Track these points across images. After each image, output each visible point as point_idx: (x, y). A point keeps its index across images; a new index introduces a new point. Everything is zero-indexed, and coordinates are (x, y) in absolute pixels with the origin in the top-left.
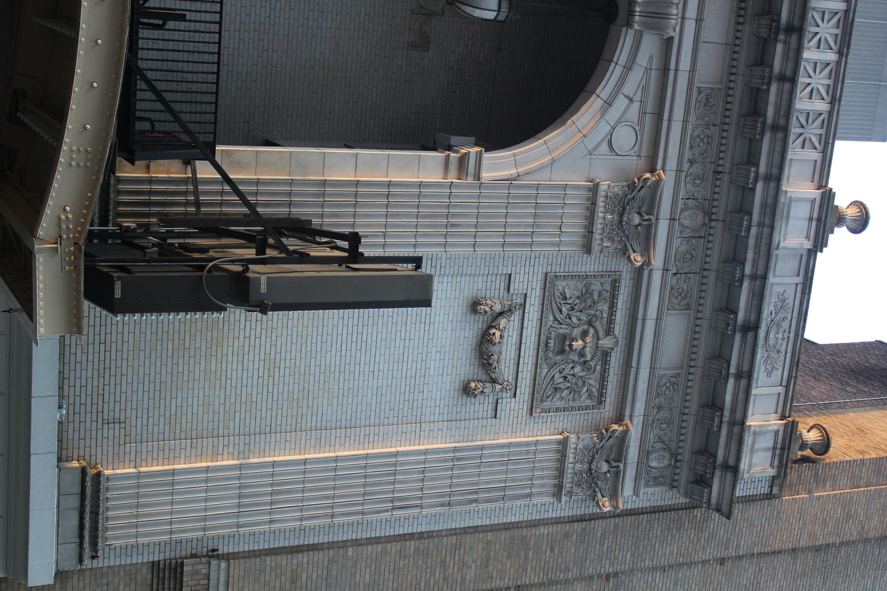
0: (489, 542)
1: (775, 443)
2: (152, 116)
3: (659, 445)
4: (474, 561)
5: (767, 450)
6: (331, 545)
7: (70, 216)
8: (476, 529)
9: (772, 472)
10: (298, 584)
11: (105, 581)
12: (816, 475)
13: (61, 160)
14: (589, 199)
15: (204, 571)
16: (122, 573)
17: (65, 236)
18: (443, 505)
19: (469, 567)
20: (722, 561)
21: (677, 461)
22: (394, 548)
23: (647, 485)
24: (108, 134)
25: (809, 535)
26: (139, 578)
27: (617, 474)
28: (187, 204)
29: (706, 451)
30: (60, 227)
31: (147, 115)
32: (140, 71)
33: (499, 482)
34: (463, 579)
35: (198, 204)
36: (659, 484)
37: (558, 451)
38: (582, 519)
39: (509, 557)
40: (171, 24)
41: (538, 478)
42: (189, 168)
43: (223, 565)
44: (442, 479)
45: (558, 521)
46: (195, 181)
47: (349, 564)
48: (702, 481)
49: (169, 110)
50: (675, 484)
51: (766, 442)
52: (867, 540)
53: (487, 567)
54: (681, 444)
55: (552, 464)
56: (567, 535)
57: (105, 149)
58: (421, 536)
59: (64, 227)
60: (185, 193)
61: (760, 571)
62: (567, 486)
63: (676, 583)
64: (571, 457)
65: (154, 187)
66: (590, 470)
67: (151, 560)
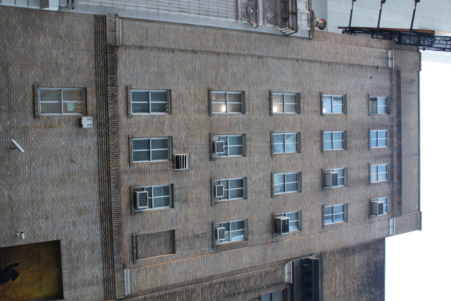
0: (215, 33)
1: (308, 18)
3: (269, 9)
4: (211, 39)
5: (306, 20)
6: (159, 22)
8: (210, 27)
9: (309, 29)
10: (148, 34)
11: (78, 19)
12: (323, 35)
14: (235, 6)
15: (114, 21)
16: (84, 17)
18: (197, 14)
19: (209, 41)
20: (297, 60)
21: (276, 15)
22: (182, 28)
23: (267, 23)
25: (325, 56)
26: (90, 20)
27: (256, 14)
29: (285, 10)
33: (216, 9)
34: (208, 45)
36: (271, 24)
37: (235, 3)
38: (247, 32)
39: (223, 40)
41: (229, 11)
43: (121, 20)
44: (196, 4)
45: (238, 31)
47: (166, 30)
48: (285, 20)
50: (277, 23)
51: (305, 17)
52: (344, 64)
53: (216, 42)
54: (277, 9)
55: (233, 7)
56: (242, 37)
58: (191, 25)
61: (311, 67)
62: (240, 16)
63: (283, 65)
64: (239, 6)
66: (247, 12)
67: (94, 14)
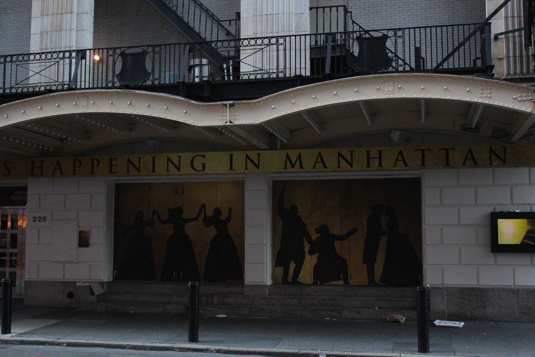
2: (473, 58)
7: (519, 95)
13: (487, 102)
17: (530, 98)
24: (472, 79)
28: (520, 36)
30: (525, 100)
31: (472, 63)
32: (438, 65)
35: (519, 30)
40: (423, 55)
42: (500, 37)
46: (507, 33)
49: (458, 48)
57: (480, 80)
59: (525, 98)
60: (514, 37)
65: (511, 54)
